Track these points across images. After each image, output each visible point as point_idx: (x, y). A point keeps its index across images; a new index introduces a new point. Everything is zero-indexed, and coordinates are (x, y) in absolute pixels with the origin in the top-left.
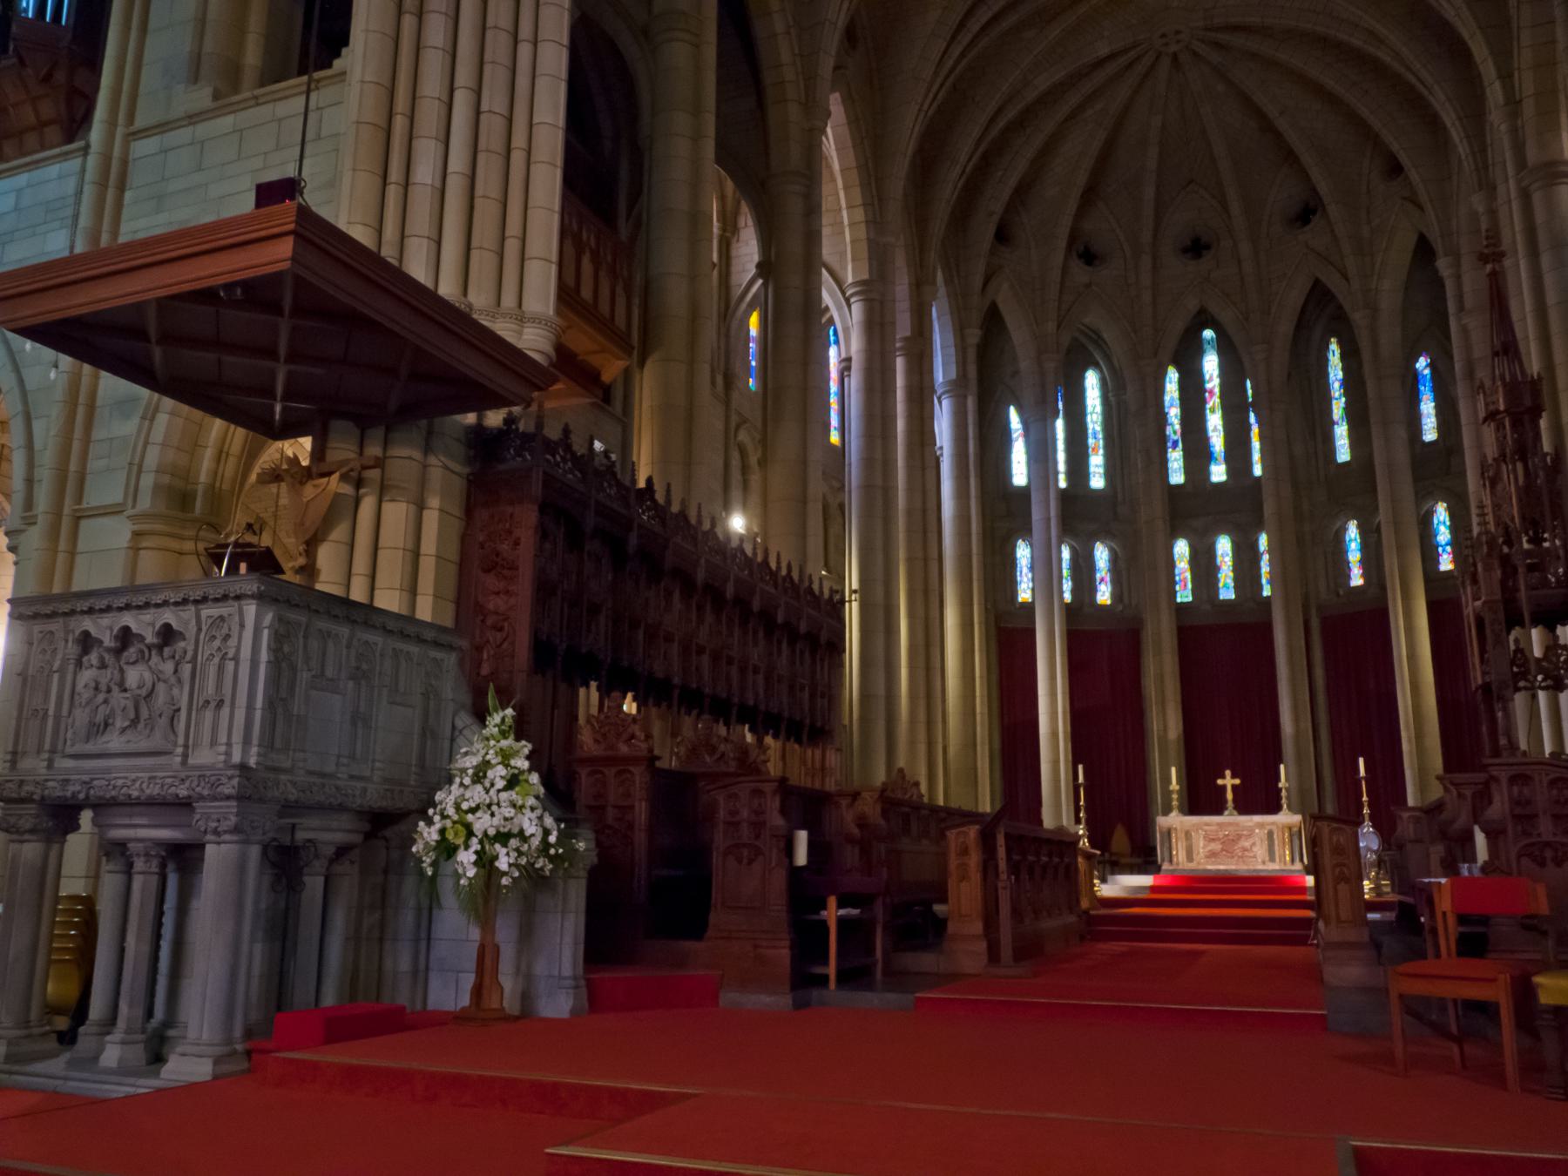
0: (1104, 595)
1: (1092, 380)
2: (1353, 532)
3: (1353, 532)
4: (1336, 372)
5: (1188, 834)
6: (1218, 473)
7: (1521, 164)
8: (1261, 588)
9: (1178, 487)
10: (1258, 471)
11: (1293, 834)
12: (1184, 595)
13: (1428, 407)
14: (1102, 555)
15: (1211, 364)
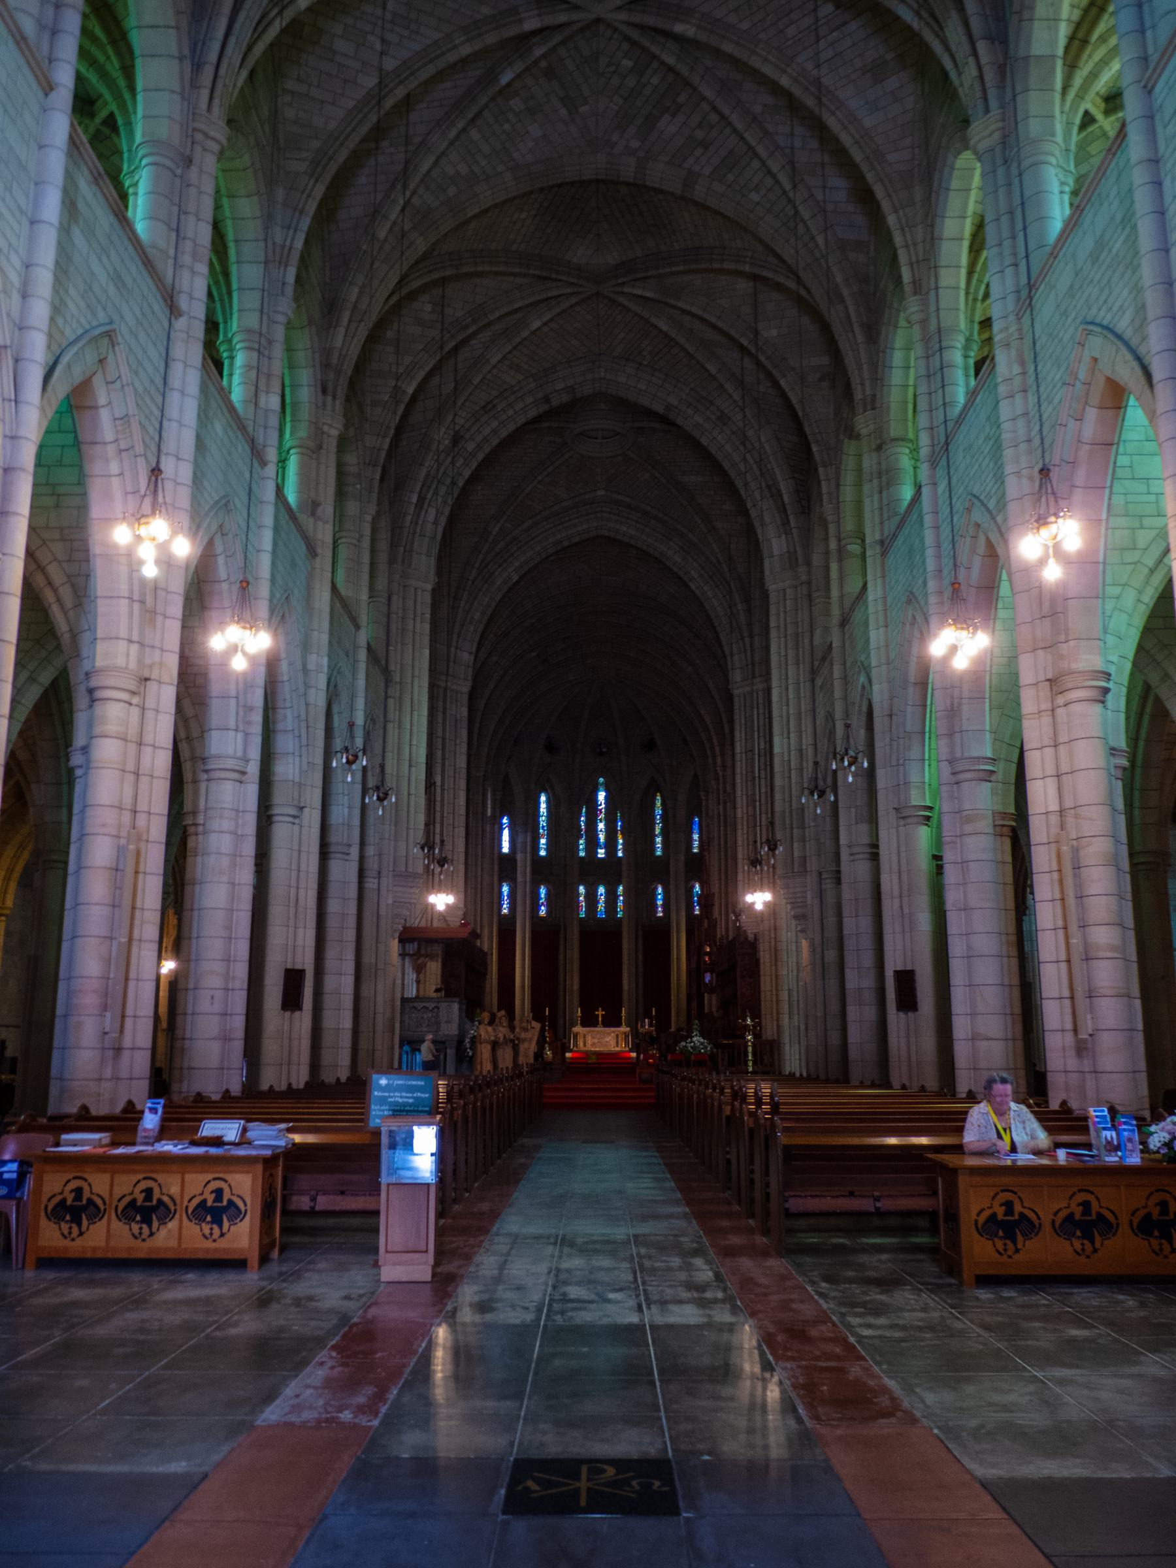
0: (543, 911)
1: (543, 798)
2: (660, 890)
3: (660, 890)
4: (659, 811)
5: (585, 1036)
6: (601, 853)
7: (725, 791)
8: (617, 913)
9: (582, 858)
10: (620, 854)
11: (626, 1036)
12: (582, 915)
13: (696, 836)
14: (543, 891)
15: (602, 796)
